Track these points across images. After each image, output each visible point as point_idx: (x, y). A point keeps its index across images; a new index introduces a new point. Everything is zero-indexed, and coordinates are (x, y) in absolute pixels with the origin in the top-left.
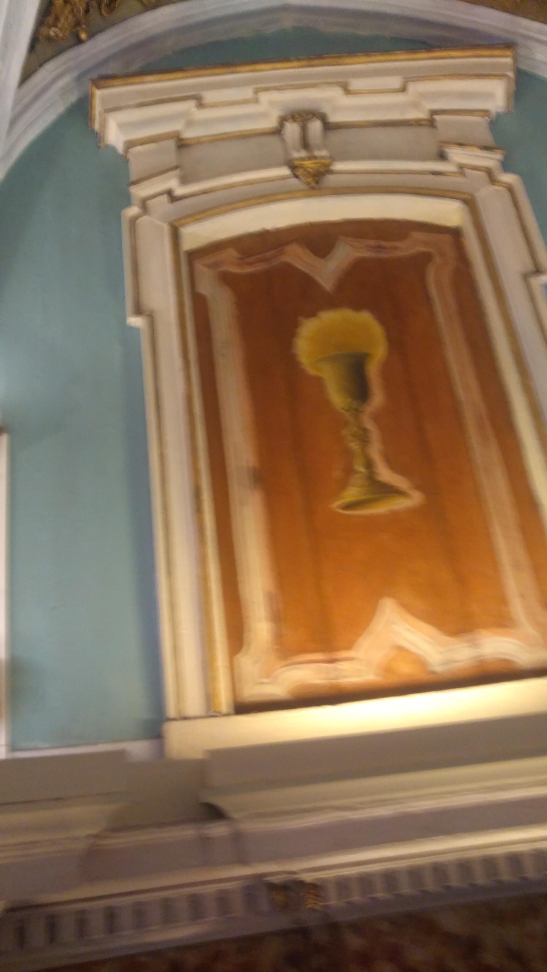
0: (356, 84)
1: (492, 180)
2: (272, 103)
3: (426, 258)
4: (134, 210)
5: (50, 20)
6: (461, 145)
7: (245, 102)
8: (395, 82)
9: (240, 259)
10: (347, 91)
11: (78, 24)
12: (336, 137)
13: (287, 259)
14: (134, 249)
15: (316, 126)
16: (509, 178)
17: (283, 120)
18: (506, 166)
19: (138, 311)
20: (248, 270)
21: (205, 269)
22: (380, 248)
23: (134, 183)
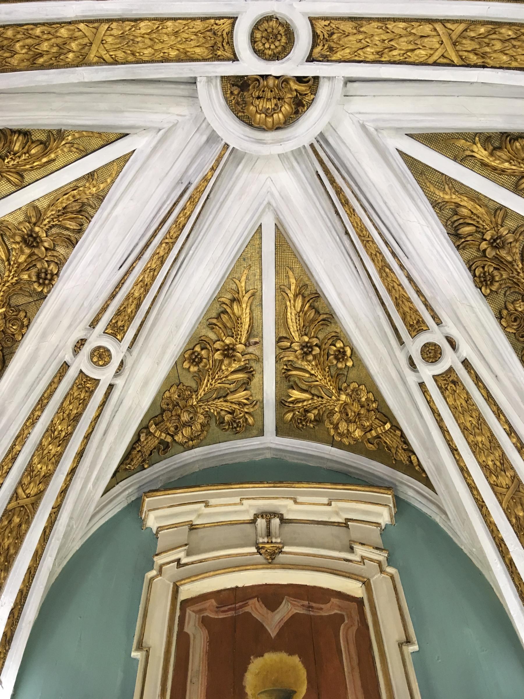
0: (300, 499)
1: (382, 571)
2: (250, 506)
3: (341, 618)
4: (154, 573)
5: (128, 461)
6: (363, 544)
7: (235, 504)
8: (325, 500)
9: (217, 607)
10: (296, 502)
11: (144, 461)
12: (288, 528)
13: (247, 609)
14: (148, 600)
15: (276, 521)
16: (391, 570)
17: (256, 516)
18: (390, 561)
19: (140, 647)
20: (221, 616)
21: (193, 614)
22: (310, 607)
23: (157, 555)
